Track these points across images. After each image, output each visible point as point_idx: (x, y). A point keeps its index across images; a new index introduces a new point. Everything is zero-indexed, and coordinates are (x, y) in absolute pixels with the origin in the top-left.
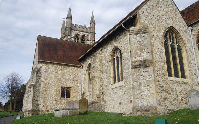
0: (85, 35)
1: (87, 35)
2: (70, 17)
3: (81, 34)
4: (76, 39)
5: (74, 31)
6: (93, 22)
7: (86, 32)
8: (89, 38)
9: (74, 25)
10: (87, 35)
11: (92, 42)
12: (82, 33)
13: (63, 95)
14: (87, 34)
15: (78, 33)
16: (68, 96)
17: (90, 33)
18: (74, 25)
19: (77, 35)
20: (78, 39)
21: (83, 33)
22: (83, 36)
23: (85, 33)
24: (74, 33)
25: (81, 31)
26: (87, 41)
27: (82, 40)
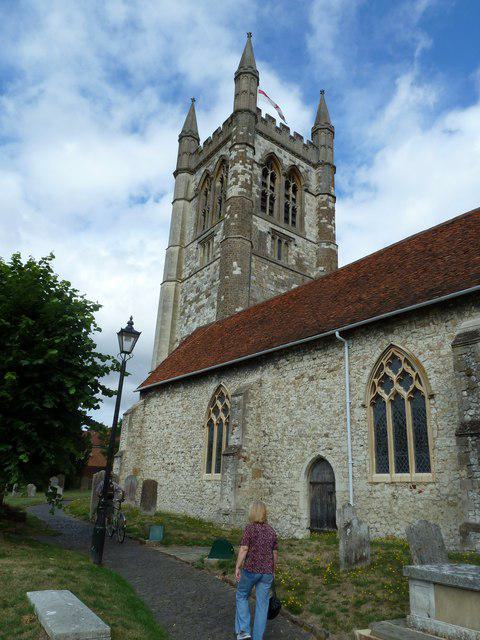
0: (301, 169)
1: (307, 171)
7: (304, 159)
8: (313, 187)
10: (307, 171)
11: (328, 200)
12: (288, 154)
15: (277, 153)
17: (315, 166)
18: (263, 116)
19: (271, 161)
20: (273, 179)
21: (294, 158)
22: (294, 171)
23: (298, 161)
24: (263, 146)
25: (288, 150)
26: (307, 195)
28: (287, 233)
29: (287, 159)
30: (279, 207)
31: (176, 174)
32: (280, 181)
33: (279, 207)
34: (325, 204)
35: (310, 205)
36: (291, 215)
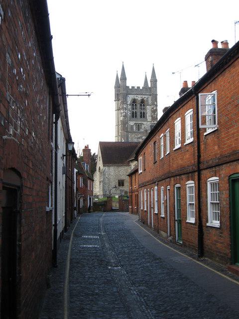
0: (145, 99)
2: (124, 78)
3: (139, 98)
4: (133, 105)
5: (130, 96)
6: (154, 81)
8: (150, 102)
9: (130, 88)
12: (140, 96)
13: (119, 185)
14: (146, 96)
16: (123, 185)
17: (150, 95)
18: (130, 88)
19: (134, 101)
20: (136, 105)
22: (143, 101)
23: (144, 96)
24: (130, 98)
27: (141, 105)
28: (140, 122)
29: (139, 98)
30: (138, 114)
31: (115, 101)
32: (138, 106)
33: (138, 114)
34: (152, 108)
35: (149, 109)
36: (143, 115)
